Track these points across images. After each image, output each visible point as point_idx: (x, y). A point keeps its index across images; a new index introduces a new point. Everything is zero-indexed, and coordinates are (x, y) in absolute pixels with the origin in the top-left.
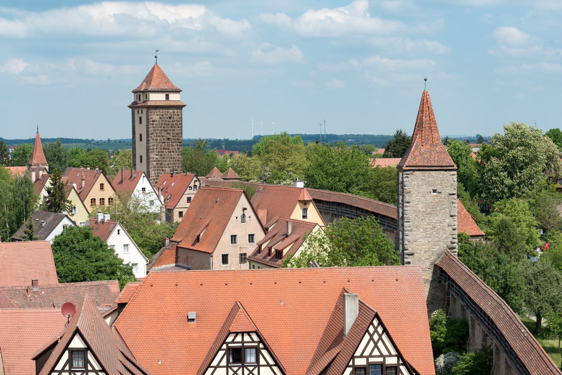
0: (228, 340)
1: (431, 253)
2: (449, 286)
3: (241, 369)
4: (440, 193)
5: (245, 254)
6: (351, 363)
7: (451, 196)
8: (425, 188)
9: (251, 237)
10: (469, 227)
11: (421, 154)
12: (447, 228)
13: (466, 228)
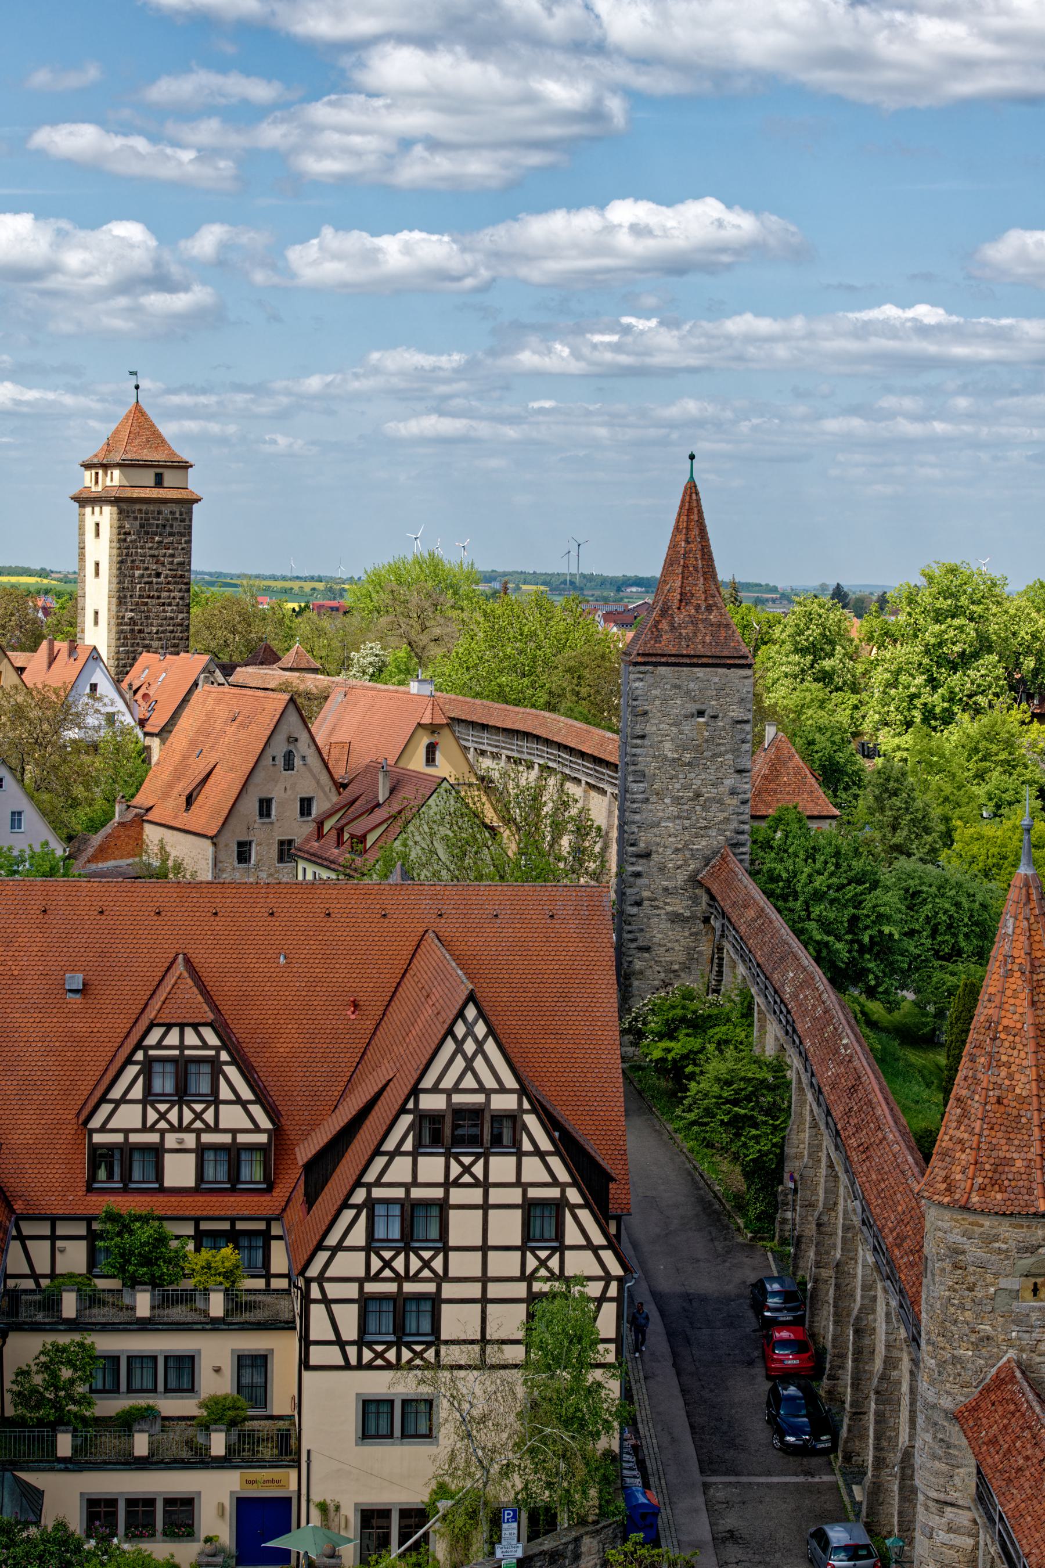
0: (147, 1042)
1: (688, 854)
2: (723, 931)
3: (176, 1108)
4: (715, 717)
5: (290, 842)
6: (410, 1105)
7: (739, 726)
8: (679, 706)
9: (306, 806)
10: (805, 796)
11: (673, 628)
13: (797, 799)
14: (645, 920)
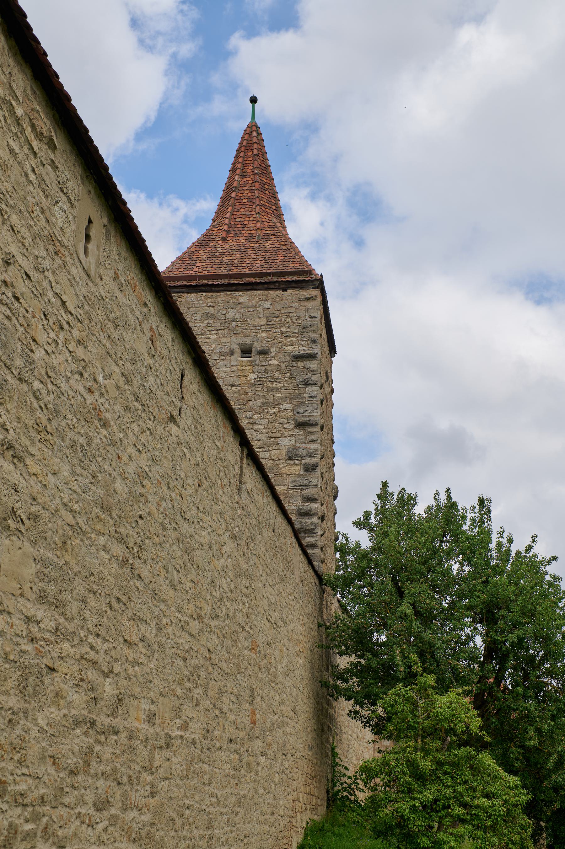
4: (264, 353)
7: (300, 364)
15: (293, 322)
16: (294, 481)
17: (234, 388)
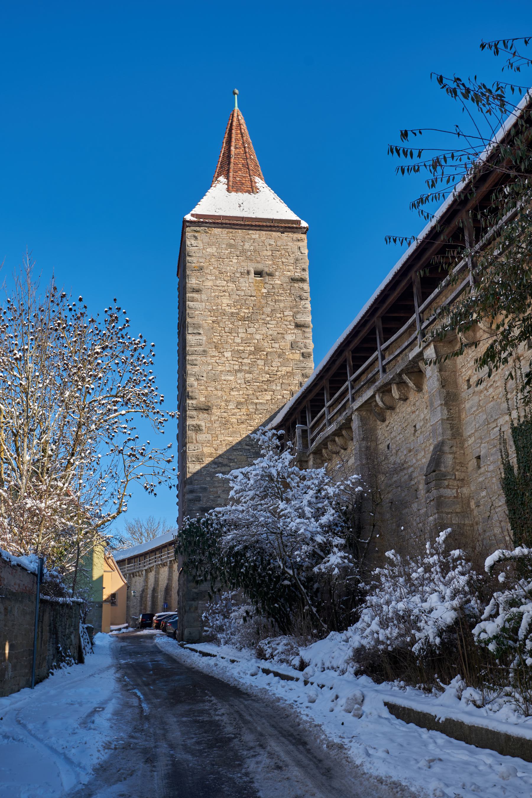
1: (251, 408)
4: (270, 275)
7: (296, 285)
12: (289, 355)
14: (208, 479)
15: (289, 255)
16: (296, 364)
17: (252, 298)
